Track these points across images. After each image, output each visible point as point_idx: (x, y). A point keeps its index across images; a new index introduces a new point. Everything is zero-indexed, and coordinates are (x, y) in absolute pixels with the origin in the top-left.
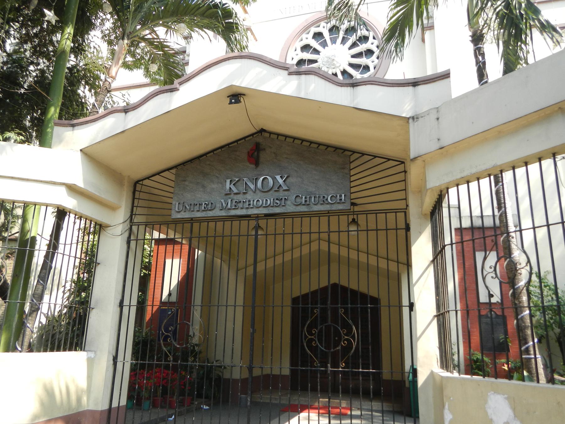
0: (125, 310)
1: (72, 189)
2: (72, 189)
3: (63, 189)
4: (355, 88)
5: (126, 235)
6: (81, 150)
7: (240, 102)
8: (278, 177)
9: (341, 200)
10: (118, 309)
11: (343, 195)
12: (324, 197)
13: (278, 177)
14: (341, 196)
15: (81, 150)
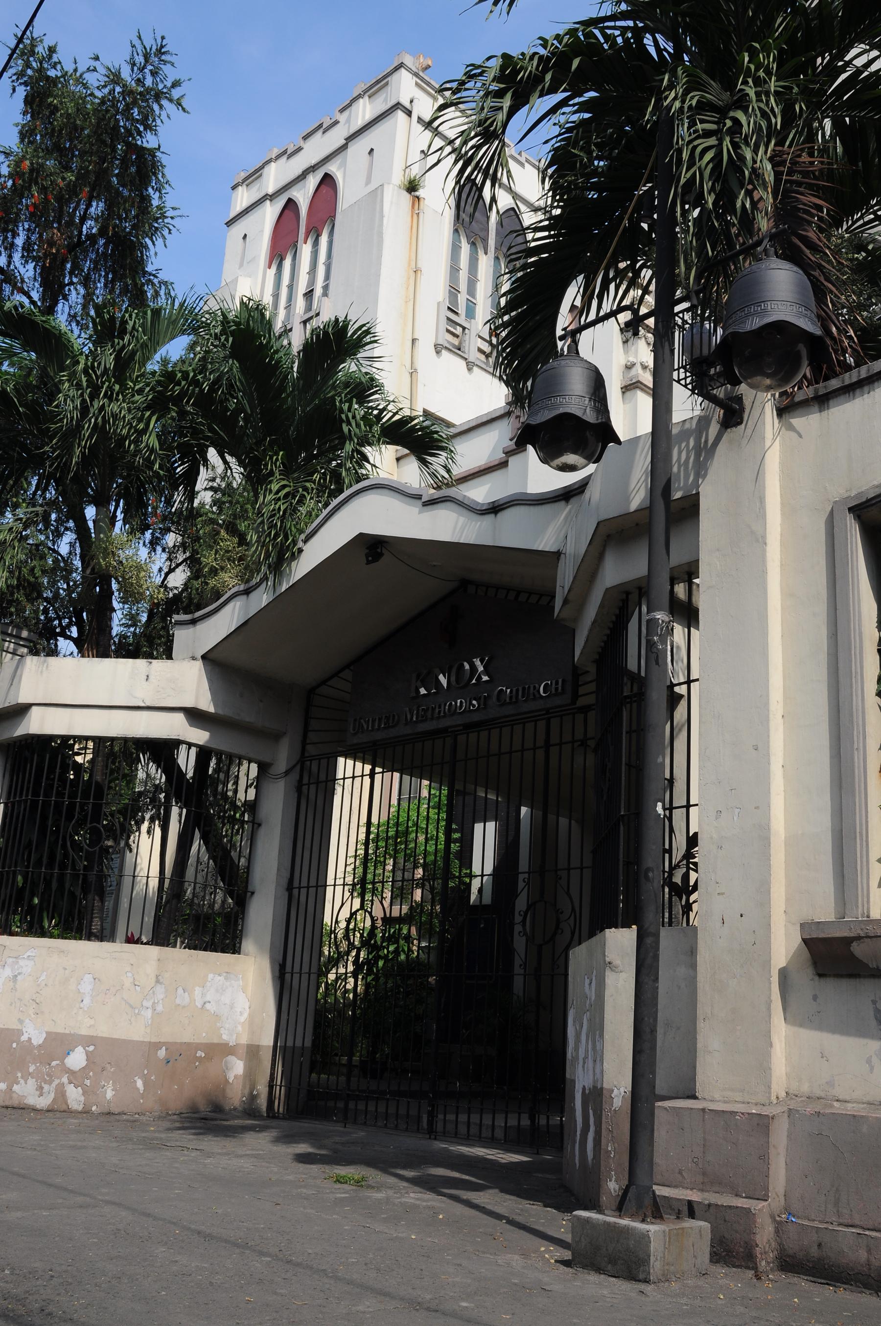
0: (296, 891)
1: (194, 715)
2: (194, 715)
3: (180, 717)
4: (500, 515)
5: (295, 776)
6: (204, 657)
7: (381, 555)
8: (477, 662)
9: (557, 689)
10: (287, 894)
11: (560, 681)
12: (535, 687)
13: (477, 662)
14: (557, 683)
15: (204, 657)
